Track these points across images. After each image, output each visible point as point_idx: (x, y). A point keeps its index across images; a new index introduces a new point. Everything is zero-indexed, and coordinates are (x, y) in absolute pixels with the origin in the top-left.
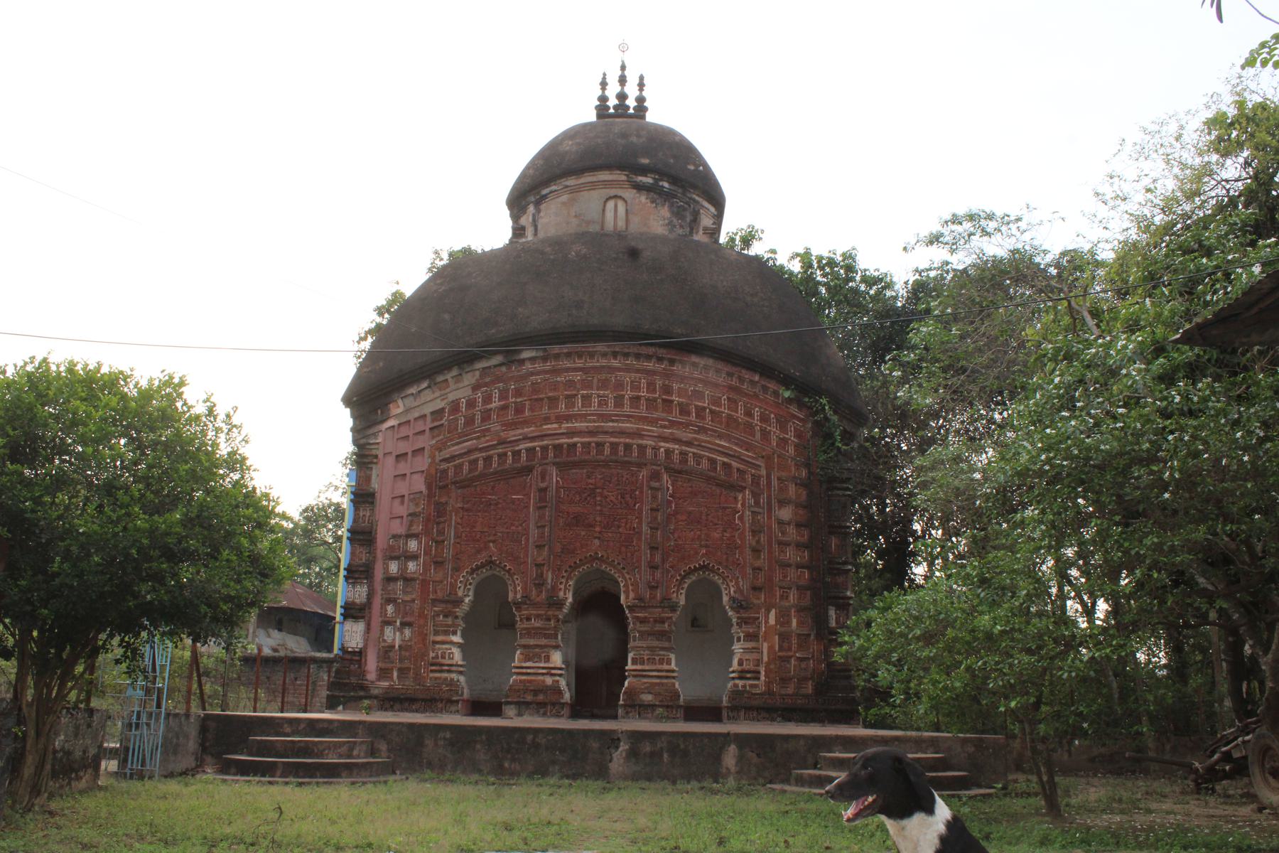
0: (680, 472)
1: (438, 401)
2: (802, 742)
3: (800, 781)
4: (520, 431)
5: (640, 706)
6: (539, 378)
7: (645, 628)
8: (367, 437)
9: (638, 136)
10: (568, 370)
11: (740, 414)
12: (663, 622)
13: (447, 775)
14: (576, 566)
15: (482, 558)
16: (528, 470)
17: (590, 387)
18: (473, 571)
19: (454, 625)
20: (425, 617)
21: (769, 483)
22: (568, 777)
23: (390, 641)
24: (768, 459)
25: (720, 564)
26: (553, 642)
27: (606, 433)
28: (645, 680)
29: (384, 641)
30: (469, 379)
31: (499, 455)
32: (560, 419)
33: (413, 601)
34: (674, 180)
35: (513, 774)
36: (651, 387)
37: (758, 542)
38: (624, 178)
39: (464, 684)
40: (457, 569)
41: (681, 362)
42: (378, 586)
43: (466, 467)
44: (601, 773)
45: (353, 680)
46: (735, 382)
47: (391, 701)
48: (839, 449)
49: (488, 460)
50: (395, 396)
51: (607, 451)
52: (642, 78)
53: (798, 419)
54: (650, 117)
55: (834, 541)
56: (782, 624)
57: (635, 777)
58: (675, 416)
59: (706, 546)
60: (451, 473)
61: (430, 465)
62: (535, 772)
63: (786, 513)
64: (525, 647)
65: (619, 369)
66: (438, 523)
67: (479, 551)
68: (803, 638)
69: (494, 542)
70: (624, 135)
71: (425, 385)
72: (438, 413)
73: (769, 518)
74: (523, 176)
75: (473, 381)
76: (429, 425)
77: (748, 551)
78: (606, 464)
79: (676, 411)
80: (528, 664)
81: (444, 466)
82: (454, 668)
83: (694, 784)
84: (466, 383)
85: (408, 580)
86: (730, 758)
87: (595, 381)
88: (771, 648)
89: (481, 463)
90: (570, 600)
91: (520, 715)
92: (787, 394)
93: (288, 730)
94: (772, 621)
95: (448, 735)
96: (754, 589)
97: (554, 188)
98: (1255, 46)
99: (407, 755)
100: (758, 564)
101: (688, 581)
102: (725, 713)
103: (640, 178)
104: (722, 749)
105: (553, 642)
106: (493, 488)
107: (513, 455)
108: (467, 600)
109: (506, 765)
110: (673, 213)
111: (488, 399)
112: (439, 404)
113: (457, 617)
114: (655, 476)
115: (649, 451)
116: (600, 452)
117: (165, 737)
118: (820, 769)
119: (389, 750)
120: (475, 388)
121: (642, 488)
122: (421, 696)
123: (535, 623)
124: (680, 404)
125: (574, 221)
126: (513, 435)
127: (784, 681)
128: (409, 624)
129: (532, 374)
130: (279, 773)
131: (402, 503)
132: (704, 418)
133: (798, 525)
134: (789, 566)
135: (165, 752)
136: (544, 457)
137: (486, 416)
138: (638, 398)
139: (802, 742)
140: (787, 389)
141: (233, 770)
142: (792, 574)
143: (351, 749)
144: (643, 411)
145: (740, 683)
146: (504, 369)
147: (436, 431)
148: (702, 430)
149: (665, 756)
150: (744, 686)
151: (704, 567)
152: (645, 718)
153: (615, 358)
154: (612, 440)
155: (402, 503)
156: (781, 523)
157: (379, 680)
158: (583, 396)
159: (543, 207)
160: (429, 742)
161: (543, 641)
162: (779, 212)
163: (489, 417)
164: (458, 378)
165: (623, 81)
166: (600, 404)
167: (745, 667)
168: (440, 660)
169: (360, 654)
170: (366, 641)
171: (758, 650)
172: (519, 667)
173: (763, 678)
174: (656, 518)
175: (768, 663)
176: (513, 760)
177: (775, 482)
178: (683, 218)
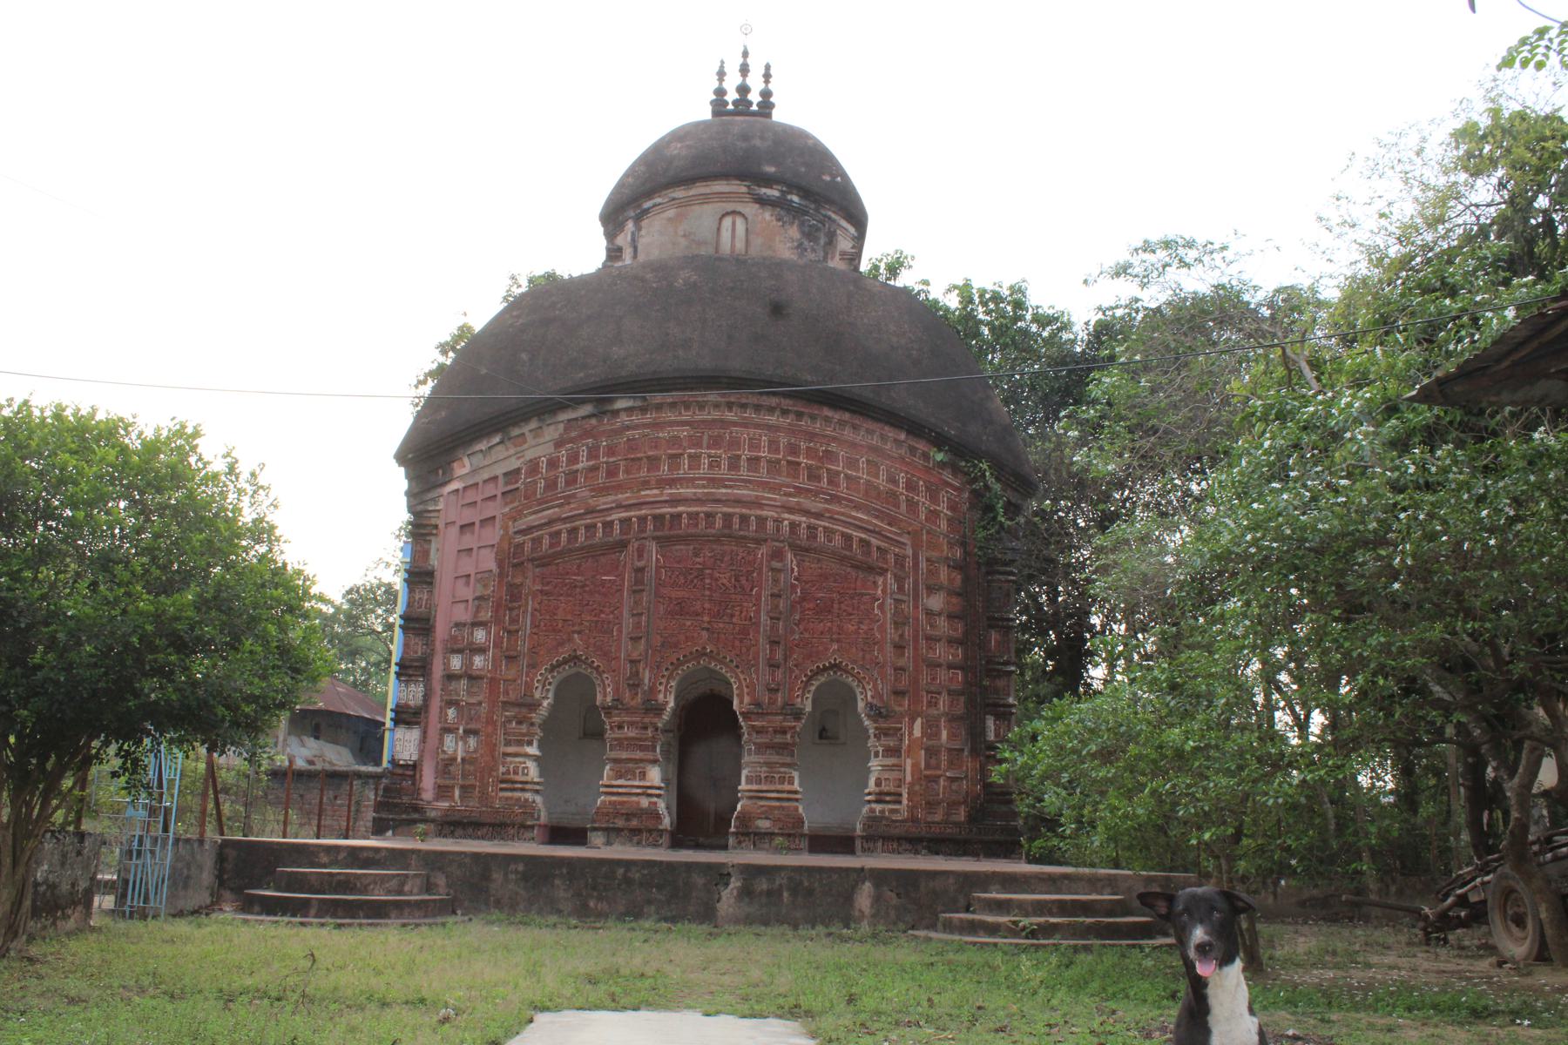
0: (807, 550)
2: (951, 881)
3: (949, 927)
5: (756, 834)
6: (636, 433)
9: (762, 138)
10: (672, 424)
11: (882, 482)
12: (784, 733)
13: (519, 917)
14: (680, 663)
16: (622, 545)
17: (699, 445)
20: (494, 723)
21: (916, 564)
22: (666, 920)
24: (915, 535)
25: (854, 662)
26: (650, 756)
30: (552, 432)
31: (587, 527)
32: (663, 483)
33: (480, 703)
34: (806, 193)
35: (601, 915)
36: (773, 446)
37: (901, 636)
38: (744, 189)
39: (540, 805)
40: (533, 666)
41: (813, 418)
42: (437, 686)
43: (546, 541)
44: (707, 914)
45: (405, 799)
46: (875, 441)
47: (452, 825)
48: (1001, 524)
49: (573, 532)
51: (719, 523)
52: (768, 67)
54: (778, 116)
55: (994, 636)
56: (930, 737)
57: (748, 920)
58: (803, 481)
60: (528, 547)
62: (627, 914)
63: (936, 602)
64: (616, 761)
65: (735, 424)
66: (511, 609)
67: (561, 644)
68: (955, 753)
70: (745, 137)
71: (497, 439)
72: (512, 475)
73: (916, 607)
74: (621, 185)
75: (556, 436)
76: (502, 488)
77: (889, 648)
78: (717, 539)
79: (804, 475)
81: (519, 539)
82: (528, 786)
83: (820, 929)
84: (548, 438)
85: (473, 678)
86: (864, 898)
87: (705, 438)
88: (913, 765)
89: (564, 536)
90: (672, 704)
91: (608, 843)
92: (940, 457)
93: (325, 859)
94: (917, 732)
95: (521, 868)
96: (898, 693)
97: (658, 200)
98: (1514, 42)
99: (468, 891)
100: (901, 663)
101: (816, 683)
102: (858, 843)
103: (764, 190)
104: (854, 888)
105: (650, 756)
106: (579, 566)
108: (545, 703)
109: (592, 904)
110: (803, 233)
111: (573, 458)
112: (514, 464)
113: (532, 724)
114: (777, 555)
115: (770, 525)
116: (710, 525)
117: (173, 868)
118: (973, 912)
119: (449, 886)
120: (559, 444)
124: (809, 467)
125: (683, 242)
126: (604, 502)
127: (931, 805)
128: (475, 732)
129: (628, 428)
130: (313, 911)
131: (468, 584)
133: (950, 617)
134: (940, 665)
135: (174, 884)
136: (642, 531)
137: (572, 479)
138: (758, 459)
139: (951, 881)
140: (940, 450)
141: (257, 908)
142: (943, 675)
143: (403, 884)
144: (763, 474)
145: (878, 807)
146: (594, 421)
147: (510, 497)
148: (835, 499)
149: (785, 894)
150: (882, 812)
153: (730, 409)
155: (468, 584)
156: (930, 613)
158: (690, 456)
159: (644, 223)
160: (497, 876)
161: (639, 755)
162: (936, 233)
163: (575, 481)
164: (537, 432)
165: (744, 70)
166: (711, 466)
167: (884, 788)
168: (512, 776)
169: (415, 767)
170: (422, 752)
171: (899, 768)
172: (608, 785)
173: (905, 802)
174: (777, 606)
175: (912, 784)
176: (600, 899)
177: (923, 565)
178: (815, 240)
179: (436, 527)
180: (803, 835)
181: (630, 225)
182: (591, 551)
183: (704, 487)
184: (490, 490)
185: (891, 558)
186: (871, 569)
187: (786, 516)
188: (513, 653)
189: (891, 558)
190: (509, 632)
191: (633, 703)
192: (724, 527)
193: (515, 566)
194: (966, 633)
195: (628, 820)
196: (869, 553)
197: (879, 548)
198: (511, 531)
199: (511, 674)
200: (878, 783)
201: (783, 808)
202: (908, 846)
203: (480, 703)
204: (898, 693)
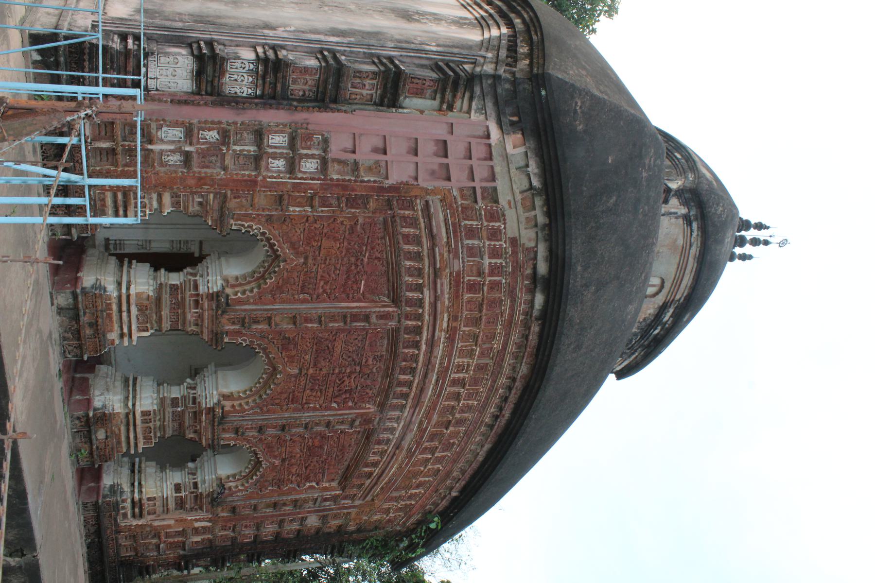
1: (510, 197)
5: (89, 432)
8: (483, 96)
10: (508, 336)
16: (396, 301)
25: (262, 476)
27: (426, 376)
28: (123, 428)
29: (160, 127)
30: (528, 237)
33: (225, 169)
49: (418, 257)
50: (531, 144)
52: (750, 257)
53: (407, 520)
61: (422, 188)
64: (158, 300)
67: (293, 246)
69: (305, 263)
71: (536, 183)
72: (492, 196)
73: (309, 512)
75: (524, 240)
78: (388, 374)
80: (134, 310)
81: (419, 205)
84: (523, 232)
85: (257, 160)
88: (169, 526)
91: (60, 310)
97: (695, 234)
103: (671, 310)
106: (378, 259)
111: (495, 253)
112: (504, 199)
115: (397, 413)
120: (514, 242)
126: (444, 283)
131: (375, 150)
133: (299, 531)
134: (258, 529)
145: (128, 504)
146: (529, 271)
150: (124, 508)
152: (74, 438)
155: (375, 150)
156: (303, 519)
159: (681, 221)
175: (151, 526)
179: (450, 108)
181: (683, 211)
182: (393, 273)
183: (440, 364)
184: (481, 172)
188: (285, 202)
190: (312, 198)
191: (224, 320)
195: (91, 325)
198: (429, 198)
202: (92, 530)
203: (225, 169)
204: (233, 510)
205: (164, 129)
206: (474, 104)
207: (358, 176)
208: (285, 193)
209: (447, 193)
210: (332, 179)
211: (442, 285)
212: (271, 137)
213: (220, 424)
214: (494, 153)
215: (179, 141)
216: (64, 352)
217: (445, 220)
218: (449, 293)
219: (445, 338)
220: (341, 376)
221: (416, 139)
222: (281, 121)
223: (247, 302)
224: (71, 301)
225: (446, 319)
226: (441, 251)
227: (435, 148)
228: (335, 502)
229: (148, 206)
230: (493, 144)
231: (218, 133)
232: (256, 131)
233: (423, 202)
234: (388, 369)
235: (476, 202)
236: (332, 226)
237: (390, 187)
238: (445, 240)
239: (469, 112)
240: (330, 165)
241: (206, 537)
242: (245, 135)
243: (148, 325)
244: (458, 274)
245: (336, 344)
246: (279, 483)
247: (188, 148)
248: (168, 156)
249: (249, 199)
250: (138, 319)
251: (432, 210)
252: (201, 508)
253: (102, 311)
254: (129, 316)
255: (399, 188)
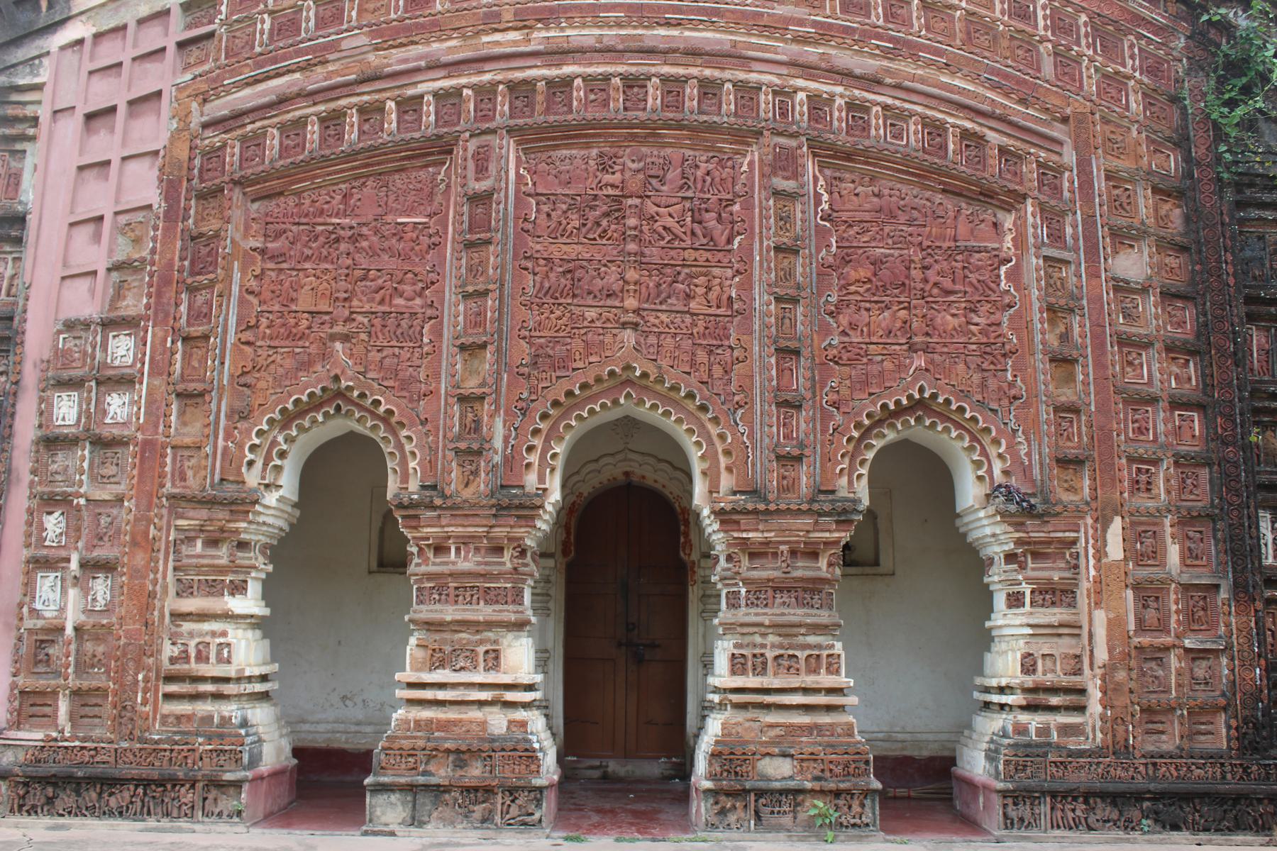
4: (420, 49)
5: (760, 793)
7: (767, 571)
12: (814, 555)
15: (311, 384)
16: (441, 148)
18: (287, 419)
19: (233, 567)
20: (150, 546)
23: (50, 613)
25: (964, 394)
26: (508, 613)
27: (651, 51)
28: (771, 718)
29: (34, 613)
33: (120, 500)
37: (1065, 337)
40: (241, 415)
43: (273, 141)
49: (332, 121)
51: (654, 96)
53: (1148, 23)
59: (927, 349)
60: (233, 154)
61: (174, 138)
66: (193, 290)
67: (306, 365)
69: (346, 338)
73: (1094, 274)
76: (177, 29)
77: (1040, 362)
78: (650, 132)
85: (101, 443)
88: (1112, 625)
89: (313, 131)
90: (555, 496)
91: (415, 821)
94: (1115, 550)
96: (1064, 462)
100: (1067, 395)
105: (508, 613)
107: (402, 112)
114: (785, 163)
115: (765, 99)
121: (749, 195)
122: (134, 772)
123: (466, 562)
128: (107, 567)
131: (97, 237)
132: (907, 23)
133: (1168, 296)
134: (1153, 400)
142: (1160, 421)
145: (1034, 721)
147: (195, 52)
148: (902, 49)
150: (1044, 731)
151: (920, 406)
152: (778, 828)
154: (666, 70)
155: (97, 237)
156: (1121, 287)
157: (17, 725)
161: (484, 612)
167: (1043, 676)
173: (1095, 707)
174: (789, 274)
175: (1109, 669)
177: (1100, 184)
179: (35, 121)
180: (867, 793)
182: (374, 163)
183: (619, 25)
185: (1030, 171)
186: (986, 195)
187: (800, 83)
189: (1030, 171)
191: (467, 494)
192: (665, 106)
193: (201, 196)
194: (1203, 330)
195: (460, 764)
196: (982, 161)
197: (1003, 150)
198: (196, 120)
199: (191, 433)
200: (1028, 666)
201: (817, 726)
203: (120, 500)
205: (38, 606)
206: (21, 82)
207: (143, 260)
208: (171, 388)
209: (187, 93)
210: (148, 307)
211: (406, 61)
212: (60, 422)
213: (765, 500)
214: (112, 25)
215: (63, 580)
216: (525, 824)
217: (248, 84)
218: (428, 42)
219: (547, 29)
220: (647, 236)
221: (81, 168)
222: (35, 407)
223: (433, 450)
224: (394, 798)
225: (498, 37)
226: (318, 79)
227: (103, 133)
228: (1063, 214)
229: (208, 639)
230: (94, 30)
231: (50, 513)
232: (48, 447)
233: (208, 133)
234: (634, 137)
235: (211, 35)
236: (267, 295)
237: (166, 200)
238: (297, 75)
239: (38, 87)
240: (122, 313)
241: (1169, 530)
242: (54, 467)
243: (481, 650)
244: (373, 34)
245: (557, 255)
246: (993, 352)
247: (74, 565)
248: (94, 600)
249: (186, 453)
250: (462, 668)
251: (225, 112)
252: (1074, 542)
253: (428, 740)
254: (455, 686)
255: (170, 181)
